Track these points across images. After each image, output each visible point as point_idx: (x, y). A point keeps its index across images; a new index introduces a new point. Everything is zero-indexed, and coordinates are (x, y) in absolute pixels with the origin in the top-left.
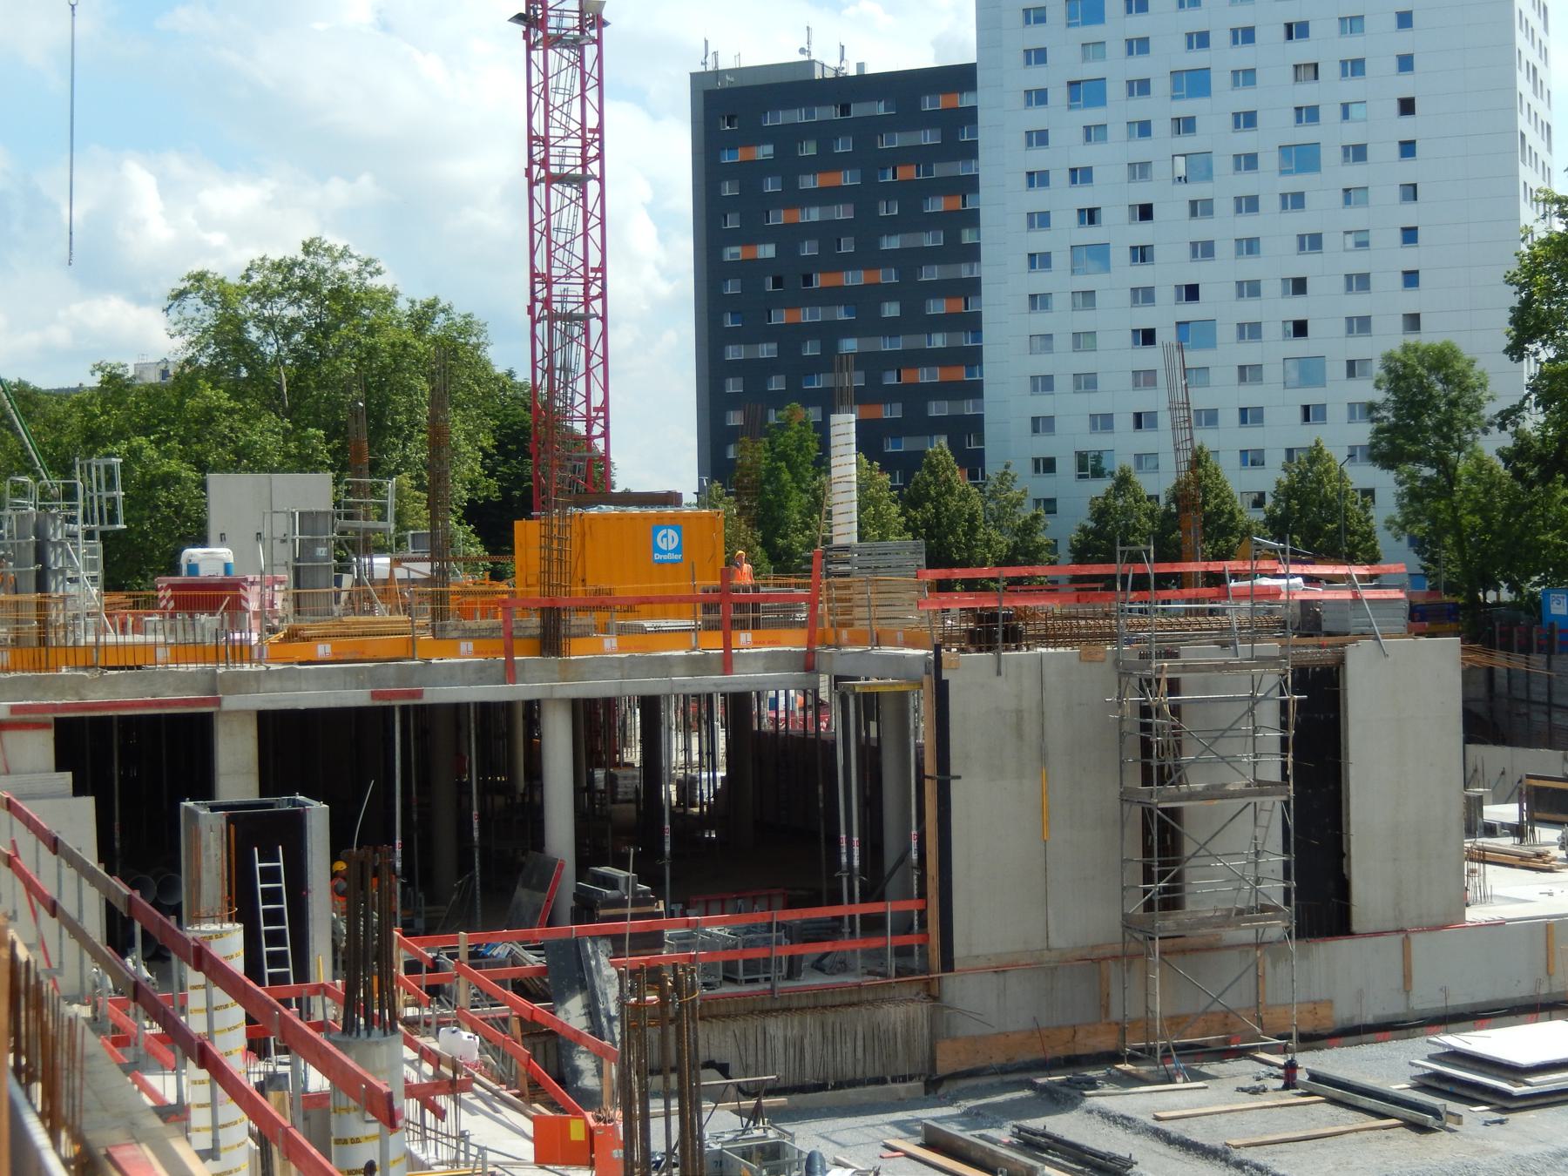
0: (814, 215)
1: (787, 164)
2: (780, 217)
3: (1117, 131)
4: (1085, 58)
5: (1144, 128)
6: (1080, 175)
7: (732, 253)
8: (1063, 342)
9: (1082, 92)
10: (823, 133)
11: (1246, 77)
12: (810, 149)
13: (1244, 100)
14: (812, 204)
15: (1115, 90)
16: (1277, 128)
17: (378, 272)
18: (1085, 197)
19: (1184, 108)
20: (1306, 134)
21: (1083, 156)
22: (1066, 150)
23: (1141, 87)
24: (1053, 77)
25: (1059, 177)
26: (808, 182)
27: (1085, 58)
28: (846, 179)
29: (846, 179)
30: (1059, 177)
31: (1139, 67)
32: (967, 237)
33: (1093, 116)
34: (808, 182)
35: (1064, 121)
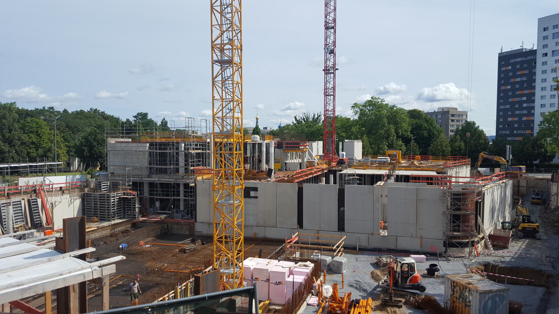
0: (519, 79)
1: (514, 70)
10: (521, 63)
12: (518, 66)
14: (518, 77)
17: (384, 101)
24: (548, 51)
25: (549, 71)
26: (519, 73)
27: (556, 45)
34: (519, 73)
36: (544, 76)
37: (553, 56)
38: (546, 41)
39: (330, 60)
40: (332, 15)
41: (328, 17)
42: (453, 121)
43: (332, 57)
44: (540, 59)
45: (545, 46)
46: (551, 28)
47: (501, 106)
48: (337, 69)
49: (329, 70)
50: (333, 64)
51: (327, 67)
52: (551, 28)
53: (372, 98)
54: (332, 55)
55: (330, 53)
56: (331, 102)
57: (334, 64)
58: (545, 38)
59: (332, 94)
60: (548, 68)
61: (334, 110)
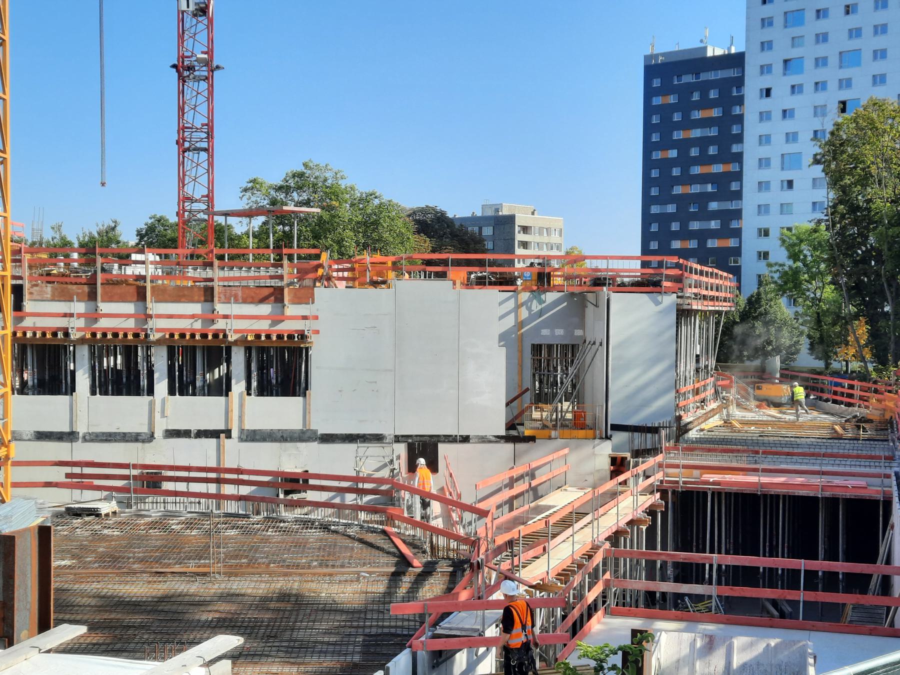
3: (809, 87)
4: (793, 46)
15: (809, 64)
19: (845, 73)
21: (790, 102)
22: (782, 99)
26: (697, 115)
28: (715, 113)
29: (715, 113)
33: (795, 79)
34: (697, 115)
35: (780, 83)
36: (764, 128)
37: (785, 74)
39: (197, 37)
42: (525, 245)
43: (201, 27)
47: (653, 207)
48: (218, 67)
50: (206, 50)
51: (183, 57)
53: (305, 165)
54: (200, 19)
55: (195, 15)
56: (201, 171)
57: (210, 52)
59: (205, 145)
61: (209, 198)
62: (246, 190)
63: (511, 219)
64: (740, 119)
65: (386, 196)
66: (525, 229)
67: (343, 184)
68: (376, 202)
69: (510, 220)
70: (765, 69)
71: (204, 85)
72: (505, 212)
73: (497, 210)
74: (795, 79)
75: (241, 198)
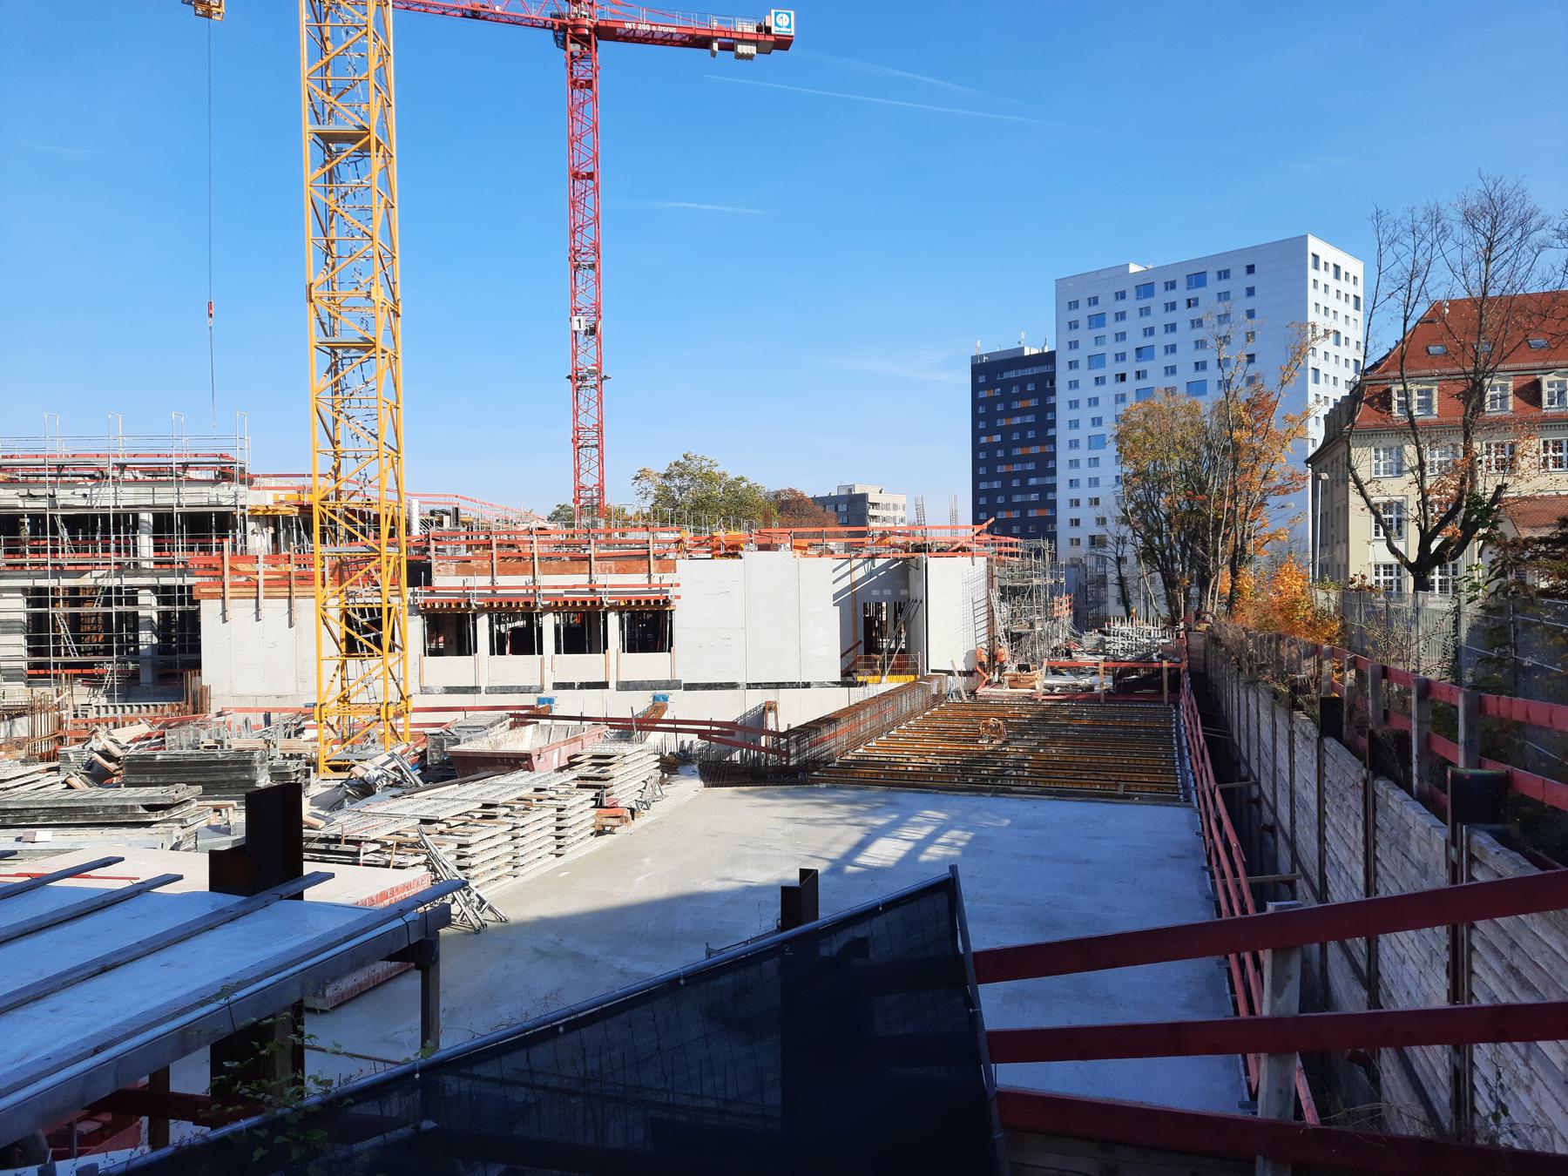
0: (1017, 420)
2: (1001, 423)
3: (1110, 379)
5: (1123, 377)
6: (1094, 402)
7: (984, 440)
8: (1084, 483)
9: (1096, 361)
10: (1022, 381)
11: (1171, 349)
13: (1170, 360)
16: (1186, 374)
18: (1095, 412)
20: (1200, 376)
22: (1088, 389)
23: (1121, 357)
24: (1080, 355)
25: (1083, 404)
30: (1083, 404)
31: (1121, 347)
32: (1051, 432)
35: (1086, 376)
36: (1074, 414)
37: (1090, 369)
38: (1075, 332)
40: (590, 231)
41: (578, 236)
44: (1063, 376)
45: (1074, 345)
46: (1083, 303)
49: (583, 379)
50: (595, 362)
52: (1083, 303)
56: (593, 464)
57: (599, 365)
58: (1073, 325)
59: (596, 442)
60: (1082, 395)
62: (637, 478)
63: (864, 497)
64: (1053, 408)
65: (752, 479)
66: (874, 505)
67: (716, 470)
68: (744, 485)
69: (864, 497)
70: (1073, 365)
71: (594, 392)
72: (857, 491)
73: (850, 490)
74: (1099, 373)
75: (633, 484)
